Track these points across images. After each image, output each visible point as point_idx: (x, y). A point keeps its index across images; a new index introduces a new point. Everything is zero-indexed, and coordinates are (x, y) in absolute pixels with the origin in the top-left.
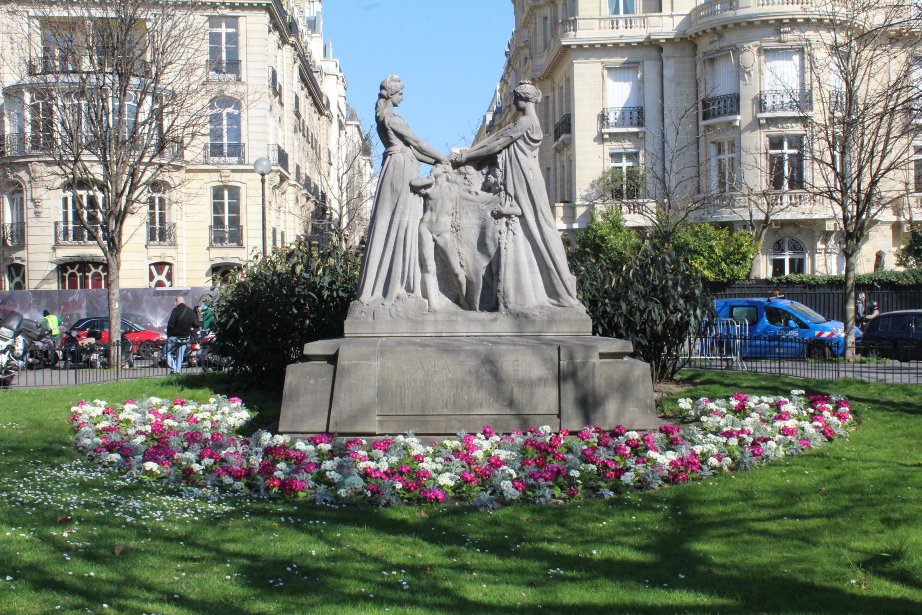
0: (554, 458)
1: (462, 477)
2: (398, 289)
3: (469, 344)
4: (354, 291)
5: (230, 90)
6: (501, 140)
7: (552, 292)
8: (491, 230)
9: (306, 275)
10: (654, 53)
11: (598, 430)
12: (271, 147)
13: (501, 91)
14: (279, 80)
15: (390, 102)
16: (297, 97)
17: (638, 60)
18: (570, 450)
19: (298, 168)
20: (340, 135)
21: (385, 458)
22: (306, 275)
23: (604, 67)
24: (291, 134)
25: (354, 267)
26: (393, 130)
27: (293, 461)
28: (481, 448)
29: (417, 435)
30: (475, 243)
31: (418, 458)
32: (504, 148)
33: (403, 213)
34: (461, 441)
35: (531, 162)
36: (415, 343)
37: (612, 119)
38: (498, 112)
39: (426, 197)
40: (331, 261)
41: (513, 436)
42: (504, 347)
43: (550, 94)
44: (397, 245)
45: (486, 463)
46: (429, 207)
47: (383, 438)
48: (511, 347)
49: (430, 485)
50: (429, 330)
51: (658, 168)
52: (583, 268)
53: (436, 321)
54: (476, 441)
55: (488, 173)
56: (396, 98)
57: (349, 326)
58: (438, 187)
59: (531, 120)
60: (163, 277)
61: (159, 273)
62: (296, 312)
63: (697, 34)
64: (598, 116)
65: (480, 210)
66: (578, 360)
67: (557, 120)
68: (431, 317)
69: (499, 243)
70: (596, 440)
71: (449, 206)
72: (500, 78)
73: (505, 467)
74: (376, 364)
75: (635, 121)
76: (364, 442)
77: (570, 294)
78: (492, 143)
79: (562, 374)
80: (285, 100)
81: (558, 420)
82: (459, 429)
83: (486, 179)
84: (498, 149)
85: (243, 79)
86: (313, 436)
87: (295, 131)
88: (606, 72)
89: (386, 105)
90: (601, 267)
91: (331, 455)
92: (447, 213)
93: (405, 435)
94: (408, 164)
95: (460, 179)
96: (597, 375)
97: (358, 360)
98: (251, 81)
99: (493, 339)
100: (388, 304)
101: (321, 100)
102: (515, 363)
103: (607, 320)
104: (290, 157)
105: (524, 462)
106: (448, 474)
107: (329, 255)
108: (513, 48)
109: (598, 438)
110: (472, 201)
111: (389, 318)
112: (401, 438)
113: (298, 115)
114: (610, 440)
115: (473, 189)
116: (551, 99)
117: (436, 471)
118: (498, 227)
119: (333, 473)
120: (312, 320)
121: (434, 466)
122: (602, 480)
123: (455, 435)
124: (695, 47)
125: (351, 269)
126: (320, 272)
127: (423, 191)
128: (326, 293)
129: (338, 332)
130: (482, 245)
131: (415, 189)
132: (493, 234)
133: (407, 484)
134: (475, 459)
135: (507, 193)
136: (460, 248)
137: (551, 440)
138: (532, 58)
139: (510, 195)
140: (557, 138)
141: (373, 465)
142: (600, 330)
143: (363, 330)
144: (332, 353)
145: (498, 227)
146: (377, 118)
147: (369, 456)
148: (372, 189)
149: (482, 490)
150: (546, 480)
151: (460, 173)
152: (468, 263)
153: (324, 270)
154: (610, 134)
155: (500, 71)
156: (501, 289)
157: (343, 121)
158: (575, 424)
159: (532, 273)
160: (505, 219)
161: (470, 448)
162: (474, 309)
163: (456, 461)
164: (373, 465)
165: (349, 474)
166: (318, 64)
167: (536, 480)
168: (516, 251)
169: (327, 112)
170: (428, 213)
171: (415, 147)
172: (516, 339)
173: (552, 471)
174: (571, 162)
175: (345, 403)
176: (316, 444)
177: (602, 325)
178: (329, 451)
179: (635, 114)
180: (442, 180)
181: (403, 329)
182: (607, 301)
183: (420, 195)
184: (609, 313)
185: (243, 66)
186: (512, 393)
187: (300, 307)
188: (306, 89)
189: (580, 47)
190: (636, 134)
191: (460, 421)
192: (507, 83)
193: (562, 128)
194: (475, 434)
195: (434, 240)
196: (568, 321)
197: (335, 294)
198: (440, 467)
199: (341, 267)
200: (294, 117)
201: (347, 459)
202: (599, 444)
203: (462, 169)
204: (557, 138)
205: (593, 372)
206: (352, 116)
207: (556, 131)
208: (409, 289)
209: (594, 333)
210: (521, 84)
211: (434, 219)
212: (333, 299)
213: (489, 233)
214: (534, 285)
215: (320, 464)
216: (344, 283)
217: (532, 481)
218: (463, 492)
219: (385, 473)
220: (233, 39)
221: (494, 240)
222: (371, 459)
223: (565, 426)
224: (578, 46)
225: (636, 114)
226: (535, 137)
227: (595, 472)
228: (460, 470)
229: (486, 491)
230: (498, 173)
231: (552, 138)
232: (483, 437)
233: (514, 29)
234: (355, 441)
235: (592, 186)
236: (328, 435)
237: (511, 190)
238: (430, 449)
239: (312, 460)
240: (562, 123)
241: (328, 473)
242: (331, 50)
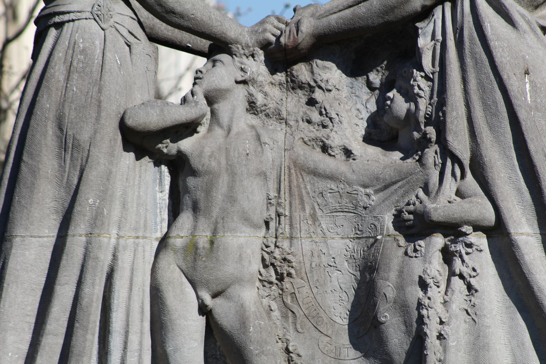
8: (393, 275)
33: (97, 221)
39: (179, 166)
46: (187, 200)
55: (387, 86)
58: (219, 132)
65: (357, 209)
69: (421, 320)
71: (255, 196)
83: (382, 102)
92: (247, 220)
94: (117, 54)
95: (294, 104)
110: (331, 177)
115: (336, 140)
118: (417, 267)
127: (168, 147)
131: (139, 141)
135: (447, 153)
136: (291, 335)
139: (456, 160)
145: (417, 267)
151: (294, 85)
170: (185, 219)
180: (233, 107)
183: (159, 160)
195: (203, 310)
203: (302, 71)
211: (203, 242)
213: (388, 287)
221: (402, 307)
230: (422, 85)
237: (460, 144)
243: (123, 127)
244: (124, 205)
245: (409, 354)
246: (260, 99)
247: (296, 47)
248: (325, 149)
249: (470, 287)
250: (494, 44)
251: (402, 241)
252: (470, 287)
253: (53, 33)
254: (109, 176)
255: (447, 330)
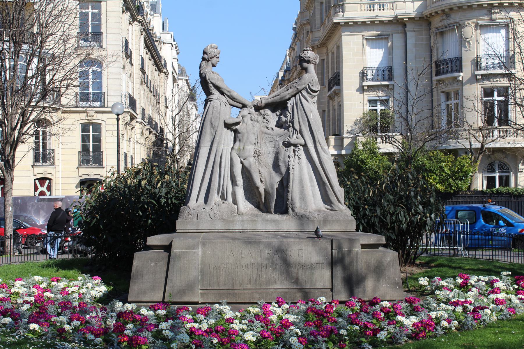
0: (328, 320)
1: (262, 335)
2: (215, 198)
3: (266, 237)
4: (184, 199)
5: (95, 54)
6: (290, 91)
7: (327, 200)
8: (282, 155)
9: (149, 187)
10: (400, 28)
11: (360, 301)
12: (124, 95)
13: (290, 55)
14: (130, 46)
15: (210, 63)
16: (143, 59)
17: (389, 33)
18: (340, 315)
19: (143, 110)
20: (174, 87)
21: (205, 321)
22: (149, 187)
23: (364, 38)
24: (138, 86)
25: (184, 182)
26: (212, 83)
27: (138, 323)
28: (275, 313)
29: (228, 303)
30: (271, 165)
31: (230, 321)
32: (292, 96)
33: (219, 143)
34: (261, 308)
35: (311, 107)
36: (227, 237)
37: (370, 75)
38: (288, 70)
39: (236, 132)
40: (167, 177)
41: (298, 304)
42: (292, 240)
43: (325, 58)
44: (215, 166)
45: (279, 324)
46: (238, 139)
47: (204, 306)
48: (297, 240)
49: (238, 340)
50: (238, 227)
51: (403, 111)
52: (349, 183)
53: (242, 221)
54: (271, 308)
55: (280, 115)
56: (214, 60)
57: (180, 225)
58: (244, 124)
59: (312, 76)
60: (44, 189)
61: (42, 186)
62: (141, 214)
63: (431, 14)
64: (360, 73)
65: (275, 141)
66: (345, 249)
67: (330, 76)
68: (239, 218)
69: (289, 165)
70: (359, 308)
71: (253, 138)
72: (289, 46)
73: (293, 327)
74: (199, 252)
75: (386, 77)
76: (190, 309)
77: (339, 202)
78: (283, 92)
79: (334, 259)
80: (134, 61)
81: (331, 293)
82: (259, 299)
83: (280, 119)
84: (288, 97)
85: (104, 46)
86: (153, 304)
87: (141, 84)
88: (365, 42)
89: (207, 65)
90: (362, 182)
91: (166, 318)
92: (251, 143)
93: (220, 304)
95: (260, 118)
96: (360, 260)
97: (186, 249)
98: (109, 48)
99: (284, 234)
100: (208, 208)
101: (160, 61)
102: (300, 252)
103: (366, 220)
104: (138, 102)
105: (307, 323)
106: (251, 332)
107: (166, 173)
108: (299, 25)
109: (360, 306)
110: (269, 134)
111: (209, 218)
112: (217, 306)
113: (143, 72)
114: (369, 307)
115: (270, 126)
116: (325, 61)
117: (242, 330)
118: (288, 153)
119: (167, 331)
120: (153, 220)
121: (241, 326)
122: (363, 337)
123: (256, 303)
124: (430, 24)
125: (182, 183)
126: (159, 185)
127: (234, 127)
128: (163, 201)
129: (172, 229)
130: (276, 166)
131: (228, 126)
132: (284, 158)
133: (221, 340)
134: (271, 321)
135: (294, 129)
136: (260, 168)
137: (326, 308)
138: (312, 32)
139: (296, 130)
140: (330, 89)
141: (196, 325)
142: (361, 228)
143: (190, 227)
144: (167, 244)
145: (288, 153)
146: (201, 75)
147: (194, 319)
148: (197, 125)
149: (276, 344)
150: (323, 337)
151: (261, 114)
152: (266, 179)
153: (162, 184)
154: (368, 86)
155: (290, 41)
156: (290, 198)
157: (176, 77)
158: (343, 297)
159: (312, 186)
160: (292, 148)
161: (267, 313)
162: (270, 212)
163: (257, 323)
164: (196, 325)
165: (179, 332)
166: (158, 35)
167: (315, 336)
168: (301, 170)
169: (164, 70)
170: (238, 143)
171: (228, 96)
172: (300, 234)
173: (327, 330)
174: (340, 106)
175: (177, 281)
176: (155, 310)
177: (363, 224)
178: (165, 315)
179: (386, 72)
180: (247, 119)
181: (219, 226)
182: (366, 207)
183: (232, 130)
184: (368, 216)
185: (104, 35)
186: (297, 273)
187: (144, 211)
188: (149, 54)
189: (347, 23)
190: (387, 86)
191: (260, 294)
192: (294, 49)
193: (335, 81)
194: (271, 303)
195: (242, 163)
196: (338, 221)
197: (170, 201)
198: (245, 327)
199: (174, 181)
200: (141, 73)
201: (178, 321)
202: (361, 311)
203: (262, 111)
204: (330, 89)
205: (357, 258)
206: (182, 73)
207: (329, 84)
208: (224, 198)
209: (357, 230)
210: (304, 50)
211: (242, 148)
212: (168, 205)
213: (281, 158)
214: (314, 195)
215: (158, 325)
216: (177, 193)
217: (312, 338)
218: (262, 345)
219: (206, 331)
220: (97, 17)
221: (284, 162)
222: (195, 321)
223: (336, 298)
224: (345, 23)
225: (387, 72)
226: (314, 89)
227: (358, 331)
228: (259, 330)
229: (279, 345)
230: (288, 114)
231: (326, 89)
232: (277, 305)
233: (299, 11)
234: (184, 308)
235: (355, 123)
236: (164, 304)
237: (297, 127)
238: (238, 314)
239: (152, 322)
240: (334, 78)
241: (164, 331)
242: (167, 26)
243: (225, 123)
244: (224, 140)
245: (286, 172)
246: (253, 117)
247: (261, 106)
248: (267, 128)
249: (299, 158)
250: (304, 106)
251: (284, 148)
252: (299, 158)
253: (209, 103)
254: (222, 133)
255: (294, 167)
